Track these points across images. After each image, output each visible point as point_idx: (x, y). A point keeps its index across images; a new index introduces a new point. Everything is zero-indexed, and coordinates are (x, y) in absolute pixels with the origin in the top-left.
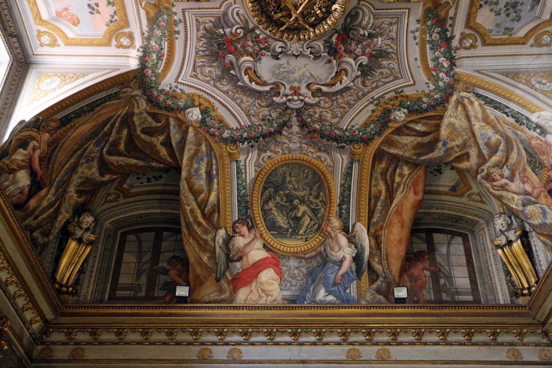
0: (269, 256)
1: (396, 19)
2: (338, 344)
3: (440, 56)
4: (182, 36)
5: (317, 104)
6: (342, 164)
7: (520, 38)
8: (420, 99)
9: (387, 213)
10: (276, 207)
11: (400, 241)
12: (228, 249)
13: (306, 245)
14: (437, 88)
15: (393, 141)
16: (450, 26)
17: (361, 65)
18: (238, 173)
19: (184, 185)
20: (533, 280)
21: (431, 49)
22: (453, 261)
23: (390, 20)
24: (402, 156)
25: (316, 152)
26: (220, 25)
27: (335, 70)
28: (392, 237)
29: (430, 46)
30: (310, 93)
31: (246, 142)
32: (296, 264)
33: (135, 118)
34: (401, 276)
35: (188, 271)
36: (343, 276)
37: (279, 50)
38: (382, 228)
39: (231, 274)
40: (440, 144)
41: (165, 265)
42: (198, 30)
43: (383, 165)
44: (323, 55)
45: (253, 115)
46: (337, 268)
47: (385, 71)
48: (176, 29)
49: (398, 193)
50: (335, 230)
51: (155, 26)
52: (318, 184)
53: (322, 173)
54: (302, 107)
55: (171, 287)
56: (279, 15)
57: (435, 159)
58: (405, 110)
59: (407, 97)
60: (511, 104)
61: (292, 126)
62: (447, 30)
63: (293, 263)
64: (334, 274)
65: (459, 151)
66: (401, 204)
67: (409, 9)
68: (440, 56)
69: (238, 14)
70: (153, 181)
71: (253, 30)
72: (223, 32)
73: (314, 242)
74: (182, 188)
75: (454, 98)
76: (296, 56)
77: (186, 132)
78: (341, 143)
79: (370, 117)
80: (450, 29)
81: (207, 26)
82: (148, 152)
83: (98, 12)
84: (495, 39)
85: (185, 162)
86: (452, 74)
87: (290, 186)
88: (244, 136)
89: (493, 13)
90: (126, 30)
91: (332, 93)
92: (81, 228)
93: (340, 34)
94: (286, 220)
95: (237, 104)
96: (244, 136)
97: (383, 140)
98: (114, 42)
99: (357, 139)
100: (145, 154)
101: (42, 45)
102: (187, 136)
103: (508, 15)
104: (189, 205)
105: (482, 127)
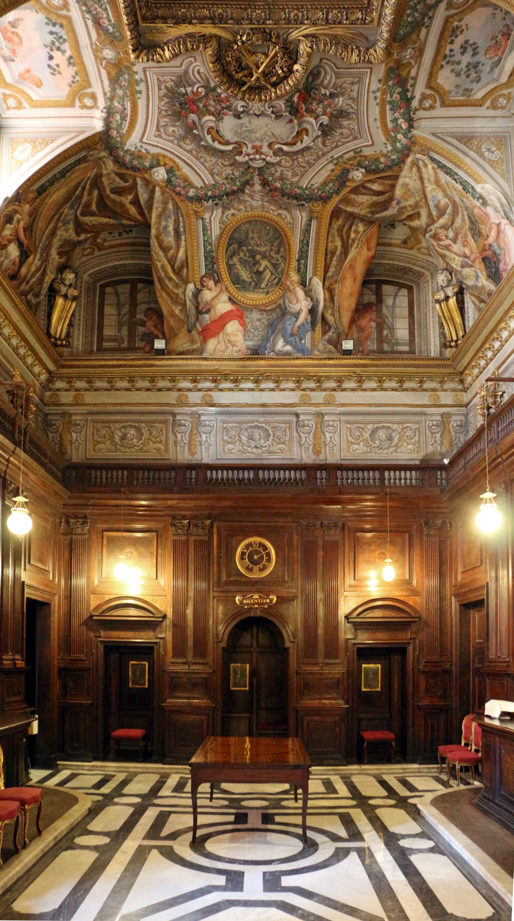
4: (144, 96)
5: (279, 164)
7: (478, 100)
8: (377, 159)
9: (341, 269)
10: (240, 262)
11: (351, 294)
12: (198, 303)
14: (395, 149)
18: (203, 231)
19: (154, 242)
20: (461, 334)
21: (391, 109)
23: (352, 80)
27: (296, 130)
28: (344, 290)
32: (258, 316)
33: (104, 179)
34: (350, 328)
35: (163, 323)
36: (299, 327)
37: (241, 109)
38: (336, 282)
39: (201, 325)
40: (394, 203)
41: (142, 317)
42: (160, 89)
43: (340, 222)
46: (295, 319)
47: (345, 131)
48: (138, 88)
51: (116, 86)
55: (150, 338)
56: (241, 75)
57: (388, 217)
58: (363, 170)
59: (365, 157)
62: (408, 90)
63: (256, 315)
66: (354, 259)
67: (371, 68)
69: (199, 72)
70: (124, 235)
71: (214, 89)
74: (152, 245)
75: (410, 160)
76: (258, 116)
77: (153, 192)
79: (329, 176)
80: (410, 89)
81: (169, 85)
82: (118, 210)
83: (60, 73)
85: (154, 220)
86: (409, 136)
87: (252, 242)
89: (454, 74)
90: (89, 91)
92: (65, 285)
98: (77, 103)
100: (116, 213)
101: (8, 108)
103: (468, 76)
104: (159, 261)
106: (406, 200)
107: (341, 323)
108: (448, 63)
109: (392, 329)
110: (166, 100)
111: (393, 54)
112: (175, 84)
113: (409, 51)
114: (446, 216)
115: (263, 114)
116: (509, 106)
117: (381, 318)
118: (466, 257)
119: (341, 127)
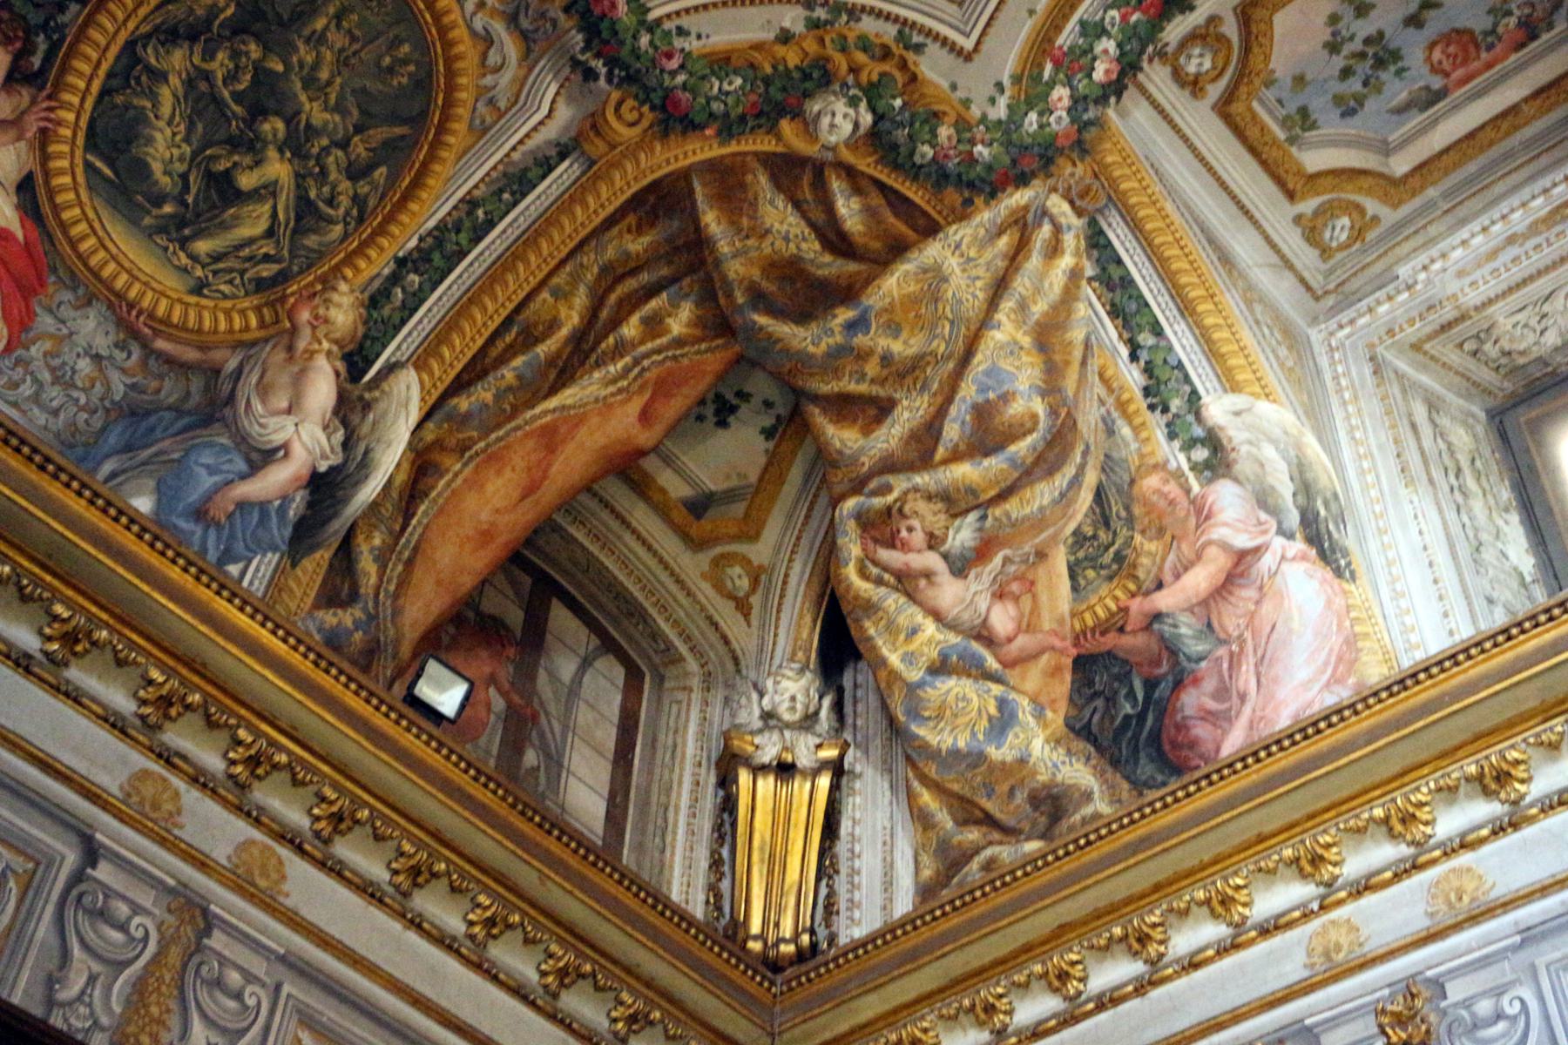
0: (20, 235)
2: (114, 722)
3: (1114, 31)
6: (535, 129)
7: (1300, 172)
8: (936, 117)
9: (515, 411)
10: (190, 84)
11: (486, 536)
13: (187, 305)
14: (1008, 128)
15: (743, 186)
22: (581, 720)
24: (717, 263)
25: (494, 13)
28: (471, 501)
32: (102, 344)
36: (243, 506)
40: (844, 315)
43: (637, 245)
46: (241, 465)
49: (596, 375)
50: (320, 333)
52: (399, 130)
53: (449, 104)
57: (786, 351)
58: (867, 119)
59: (914, 78)
60: (1181, 327)
63: (92, 328)
64: (217, 478)
65: (873, 381)
66: (574, 419)
68: (1114, 31)
73: (221, 317)
75: (1019, 198)
78: (598, 55)
79: (758, 47)
84: (1254, 116)
86: (1091, 114)
87: (305, 53)
89: (1326, 35)
94: (181, 159)
97: (723, 157)
99: (653, 82)
105: (1014, 348)
106: (894, 329)
107: (397, 612)
109: (555, 762)
114: (994, 464)
116: (1339, 256)
117: (529, 703)
118: (984, 635)
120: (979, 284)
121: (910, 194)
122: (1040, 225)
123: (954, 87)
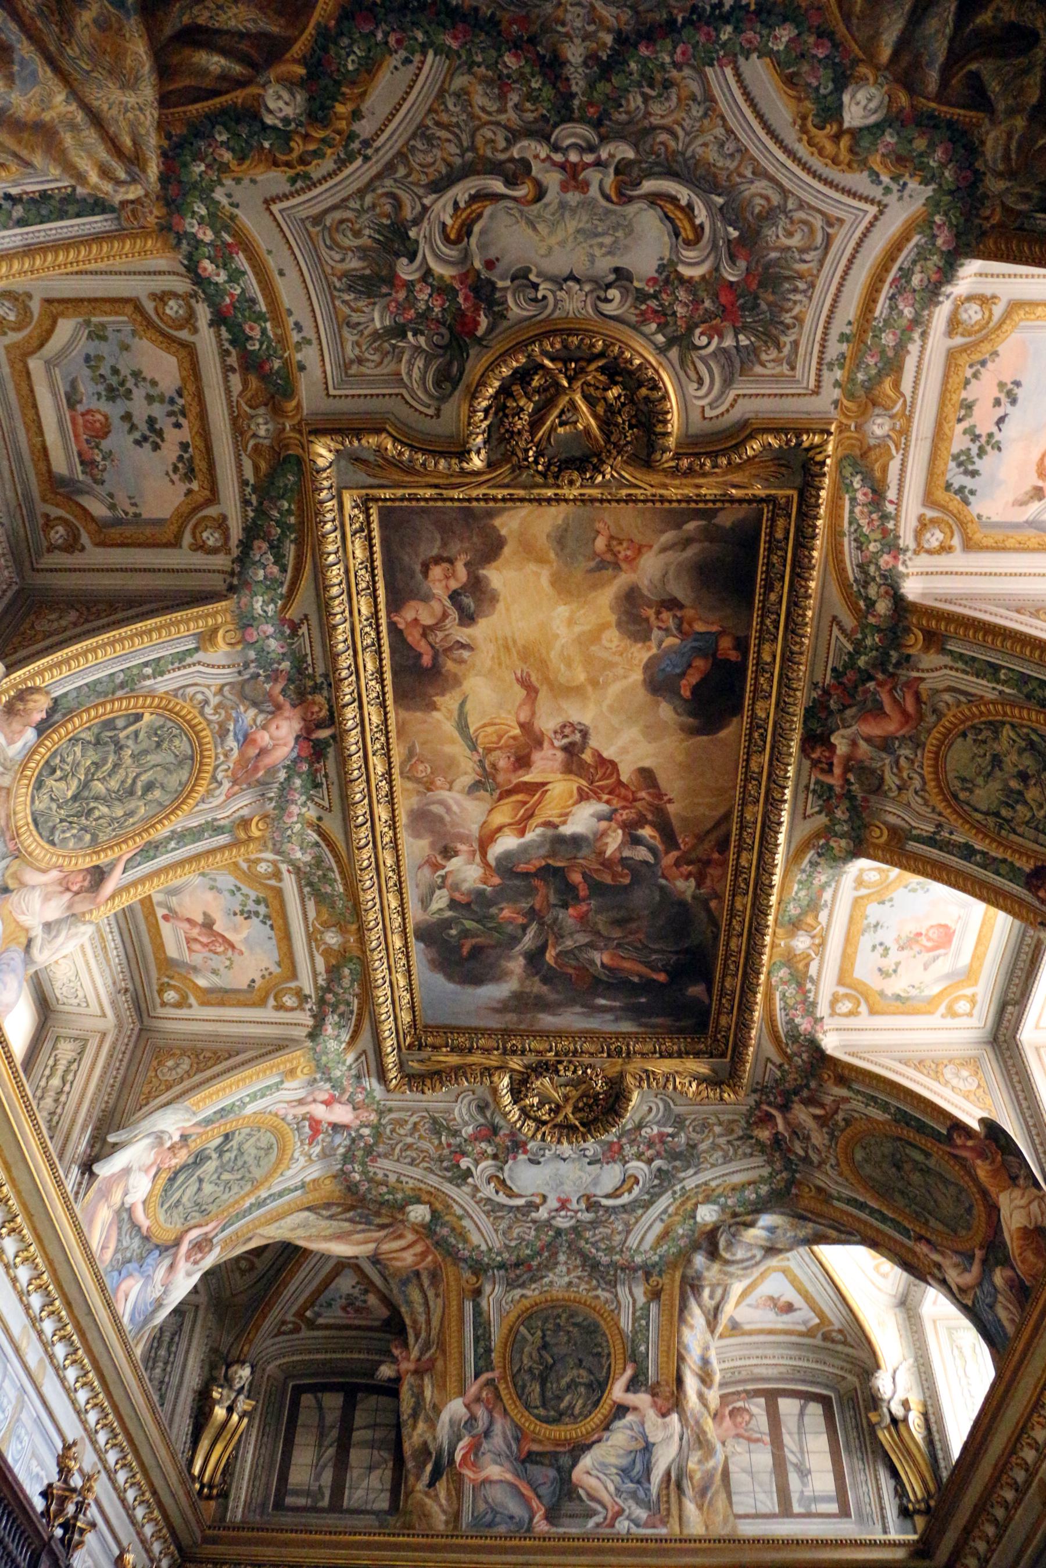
1: (351, 372)
4: (839, 326)
5: (514, 136)
7: (62, 314)
8: (241, 160)
15: (280, 13)
16: (227, 353)
17: (412, 256)
21: (253, 301)
26: (744, 355)
27: (473, 240)
29: (257, 308)
30: (534, 173)
31: (727, 7)
37: (614, 293)
42: (796, 344)
44: (508, 283)
45: (694, 98)
47: (349, 241)
48: (844, 347)
51: (891, 354)
54: (556, 125)
58: (269, 120)
59: (276, 164)
60: (18, 241)
61: (585, 64)
62: (232, 342)
69: (700, 382)
71: (671, 342)
72: (741, 337)
75: (153, 170)
76: (571, 277)
77: (903, 44)
79: (363, 95)
80: (227, 345)
81: (774, 354)
83: (1001, 385)
84: (117, 314)
86: (184, 245)
88: (729, 29)
89: (147, 374)
91: (478, 173)
93: (472, 334)
95: (737, 138)
96: (729, 29)
97: (310, 17)
99: (391, 18)
102: (903, 32)
105: (45, 103)
108: (172, 401)
110: (787, 318)
111: (293, 429)
112: (757, 356)
113: (262, 432)
115: (560, 281)
119: (363, 252)
120: (105, 107)
121: (198, 106)
122: (127, 172)
123: (253, 181)
